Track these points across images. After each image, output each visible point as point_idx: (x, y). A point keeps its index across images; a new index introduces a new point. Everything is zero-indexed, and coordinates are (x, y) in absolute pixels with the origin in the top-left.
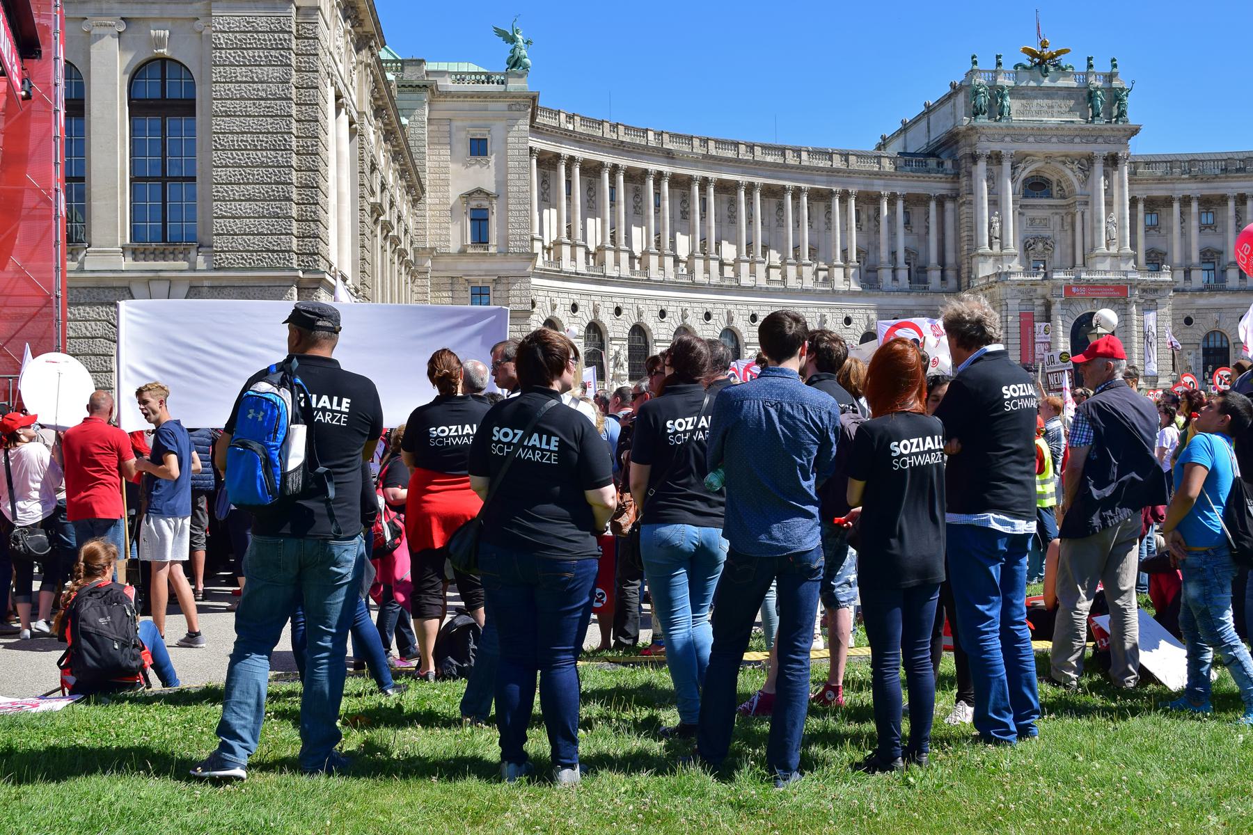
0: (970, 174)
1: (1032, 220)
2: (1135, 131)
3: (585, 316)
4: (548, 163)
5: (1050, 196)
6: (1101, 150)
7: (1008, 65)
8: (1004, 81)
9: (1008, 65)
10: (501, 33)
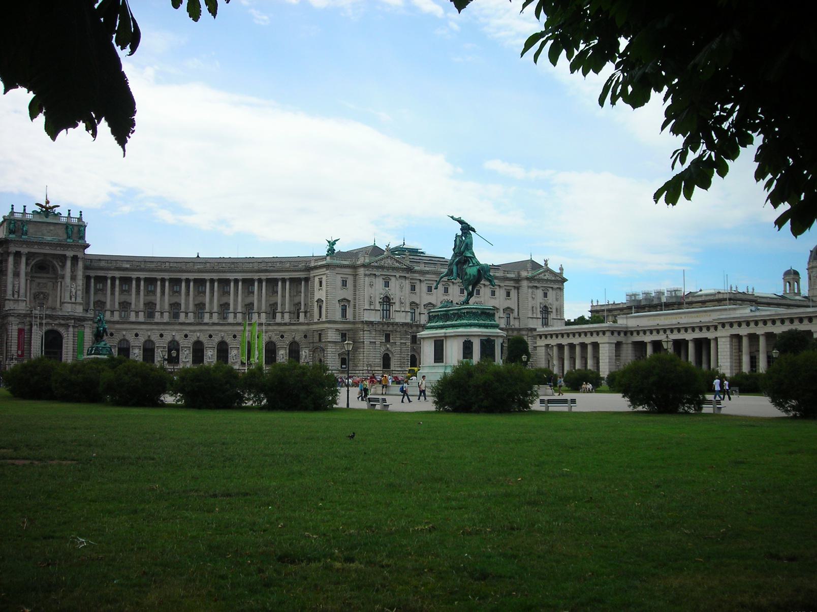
0: (7, 261)
1: (39, 284)
2: (88, 246)
5: (48, 273)
6: (70, 253)
9: (29, 211)
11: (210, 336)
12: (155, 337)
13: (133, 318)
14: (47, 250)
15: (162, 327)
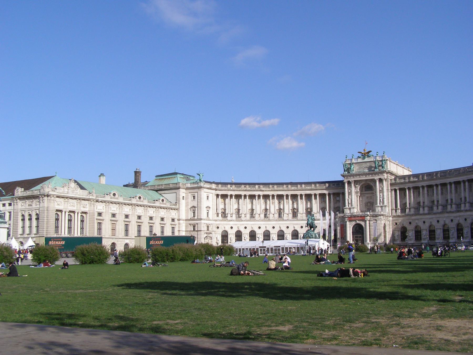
1: (367, 197)
3: (235, 230)
4: (224, 197)
7: (355, 157)
8: (354, 161)
10: (198, 174)
11: (466, 220)
12: (435, 223)
13: (421, 211)
14: (364, 178)
15: (438, 216)
